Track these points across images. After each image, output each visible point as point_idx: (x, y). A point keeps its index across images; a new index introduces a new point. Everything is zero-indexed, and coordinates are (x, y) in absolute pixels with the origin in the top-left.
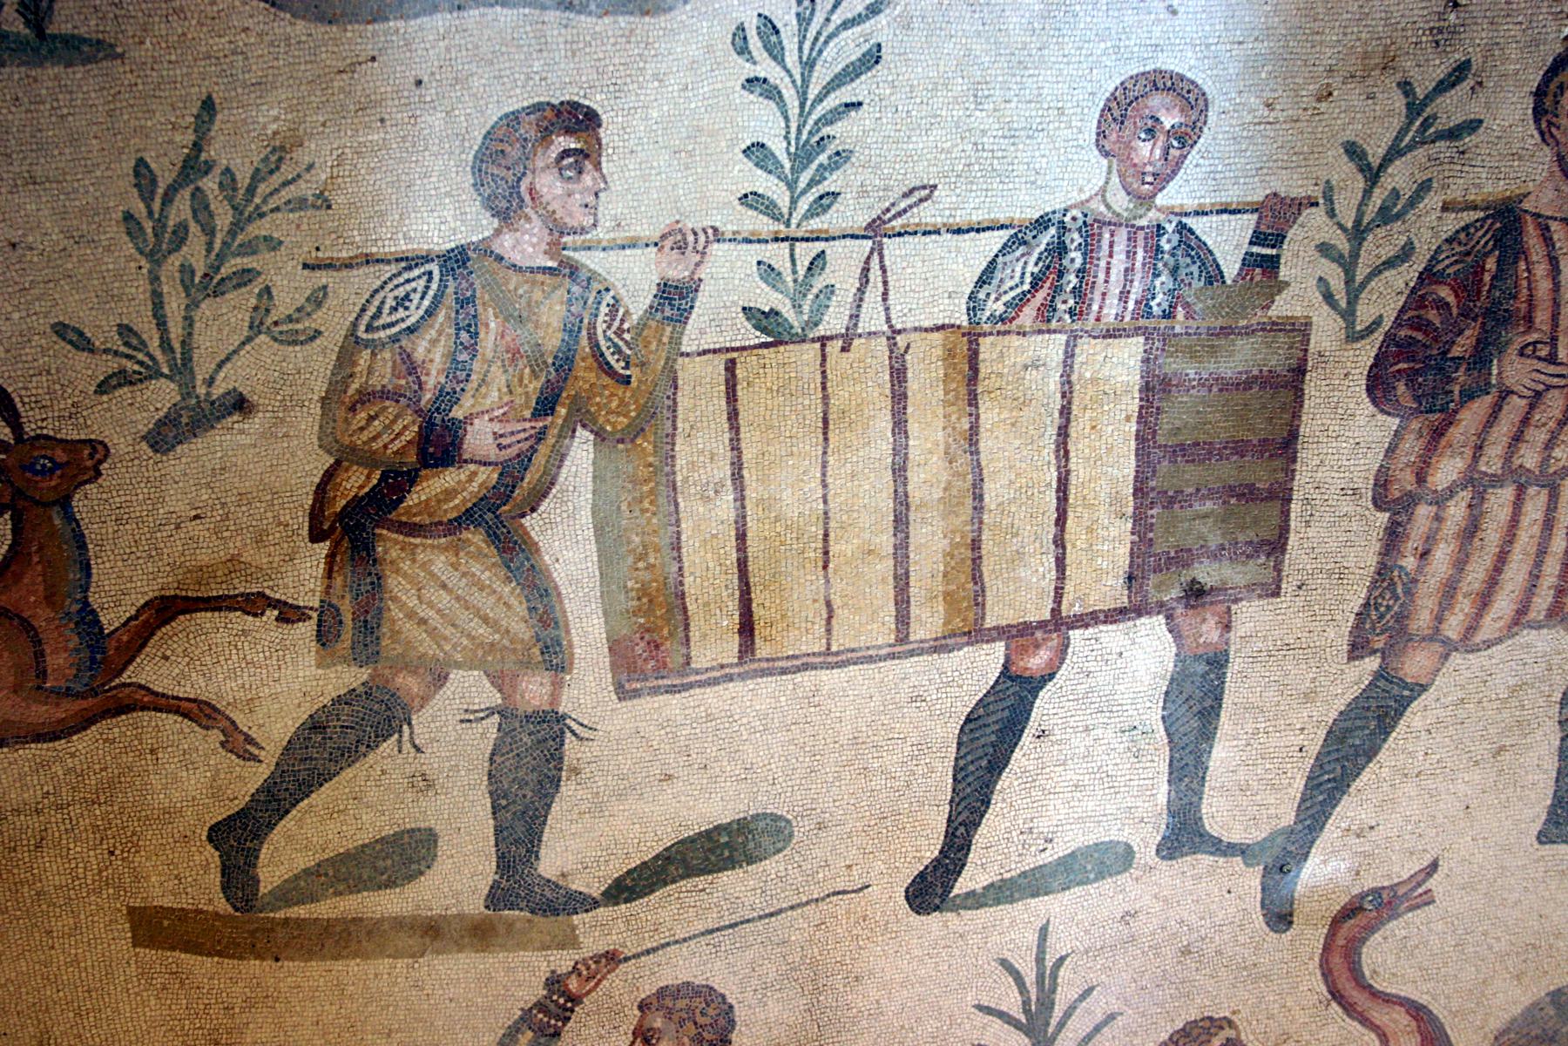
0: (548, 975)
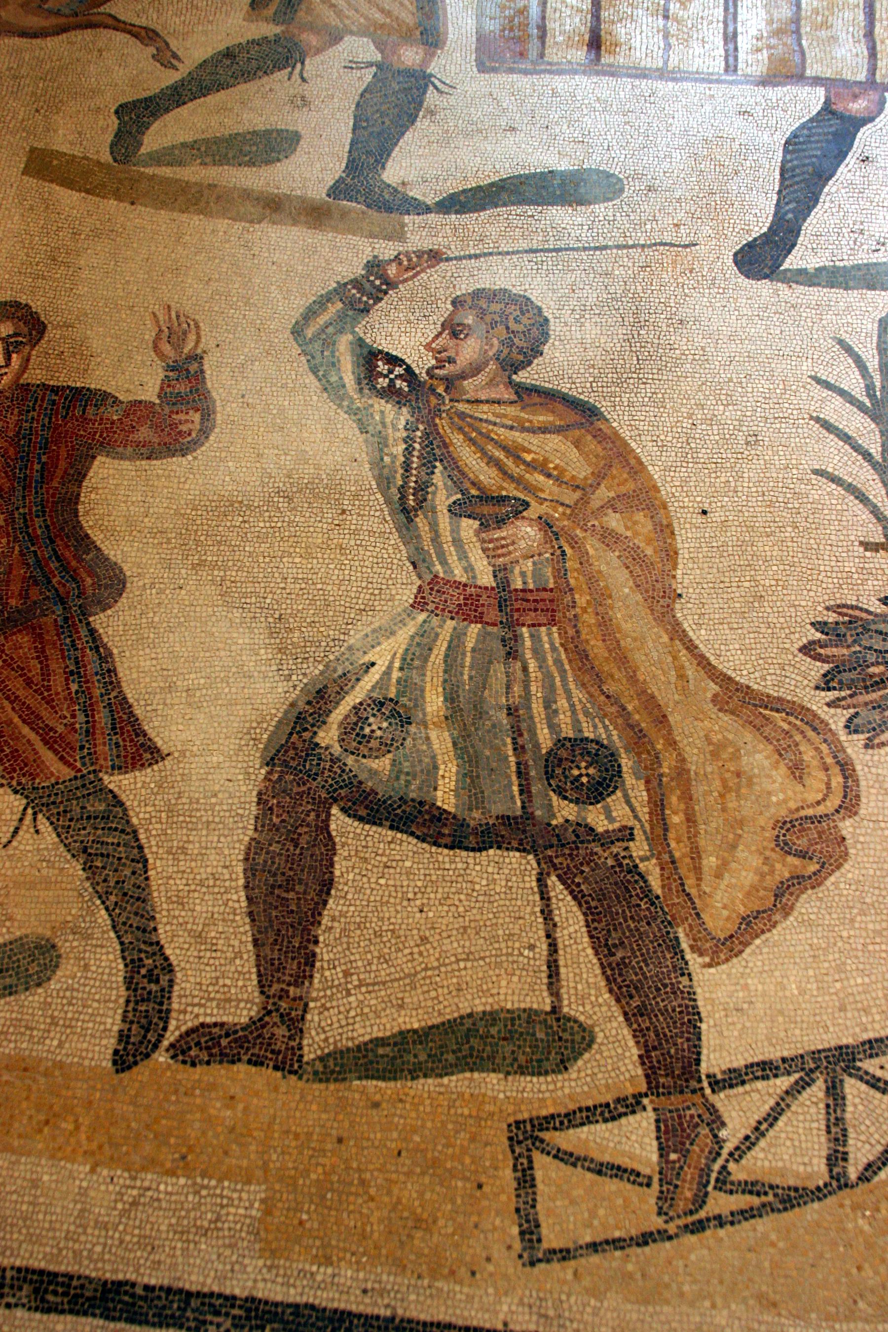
0: (370, 258)
